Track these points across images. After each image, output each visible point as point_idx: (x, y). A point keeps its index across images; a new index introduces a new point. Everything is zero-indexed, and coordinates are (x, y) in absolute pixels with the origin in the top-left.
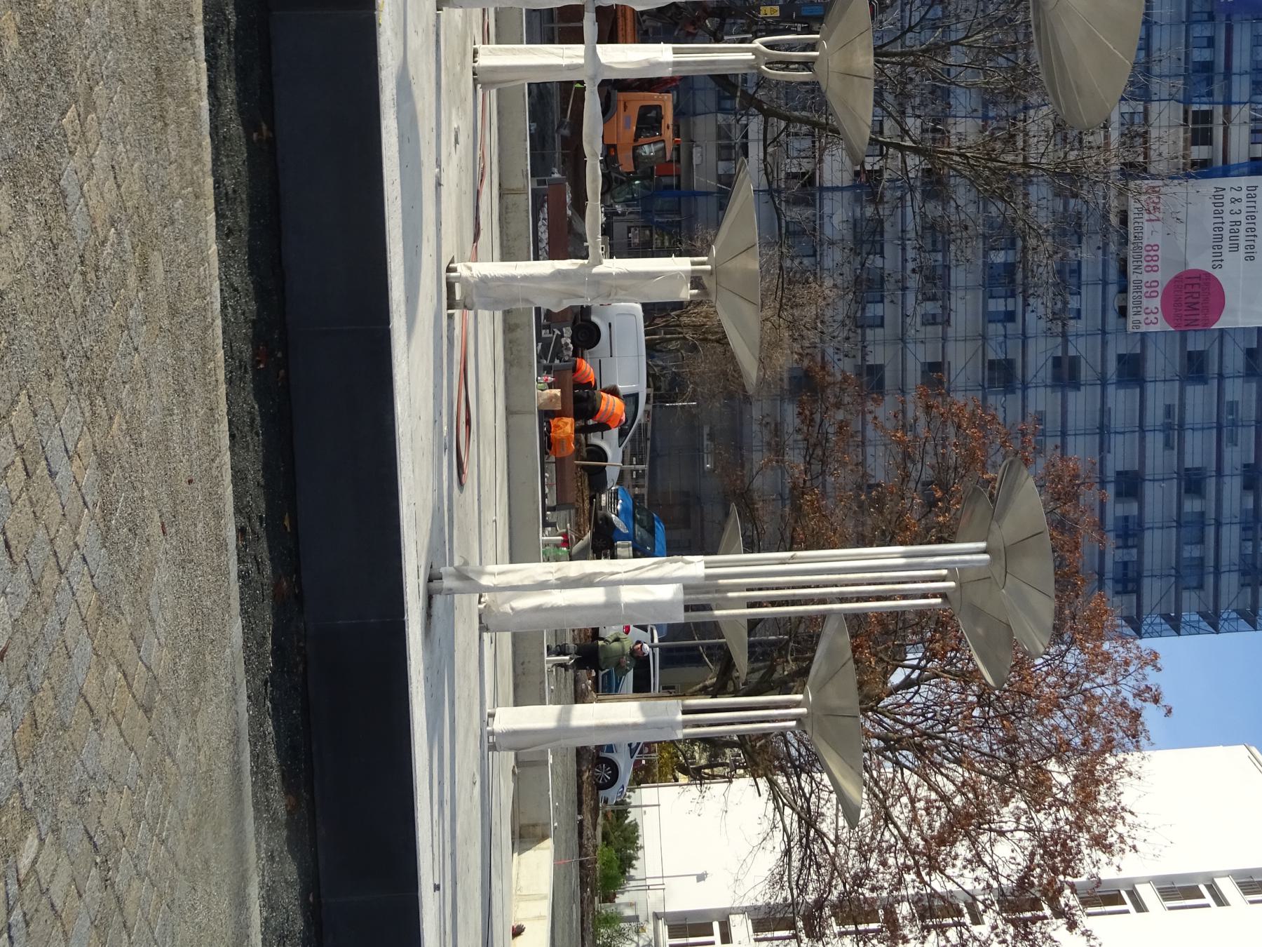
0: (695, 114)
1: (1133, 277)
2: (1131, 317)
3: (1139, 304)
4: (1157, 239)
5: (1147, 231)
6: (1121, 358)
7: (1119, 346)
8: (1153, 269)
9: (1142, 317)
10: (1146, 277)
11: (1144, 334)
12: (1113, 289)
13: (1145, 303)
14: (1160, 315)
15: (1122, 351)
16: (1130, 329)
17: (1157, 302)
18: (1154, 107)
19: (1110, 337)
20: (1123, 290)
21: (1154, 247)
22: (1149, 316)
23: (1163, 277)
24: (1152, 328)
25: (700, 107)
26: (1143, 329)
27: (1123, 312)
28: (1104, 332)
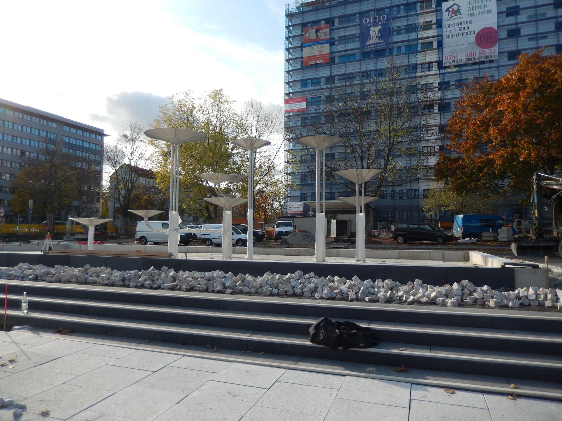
0: (419, 205)
1: (478, 60)
2: (492, 58)
3: (488, 56)
4: (464, 54)
5: (462, 57)
6: (509, 60)
7: (505, 61)
8: (475, 53)
9: (493, 55)
10: (477, 56)
11: (499, 53)
12: (482, 66)
13: (487, 54)
14: (492, 49)
15: (507, 59)
16: (497, 58)
17: (487, 51)
18: (418, 62)
19: (500, 64)
20: (483, 63)
21: (467, 54)
22: (492, 52)
23: (478, 50)
24: (497, 51)
25: (416, 204)
26: (497, 53)
27: (491, 62)
28: (498, 67)
